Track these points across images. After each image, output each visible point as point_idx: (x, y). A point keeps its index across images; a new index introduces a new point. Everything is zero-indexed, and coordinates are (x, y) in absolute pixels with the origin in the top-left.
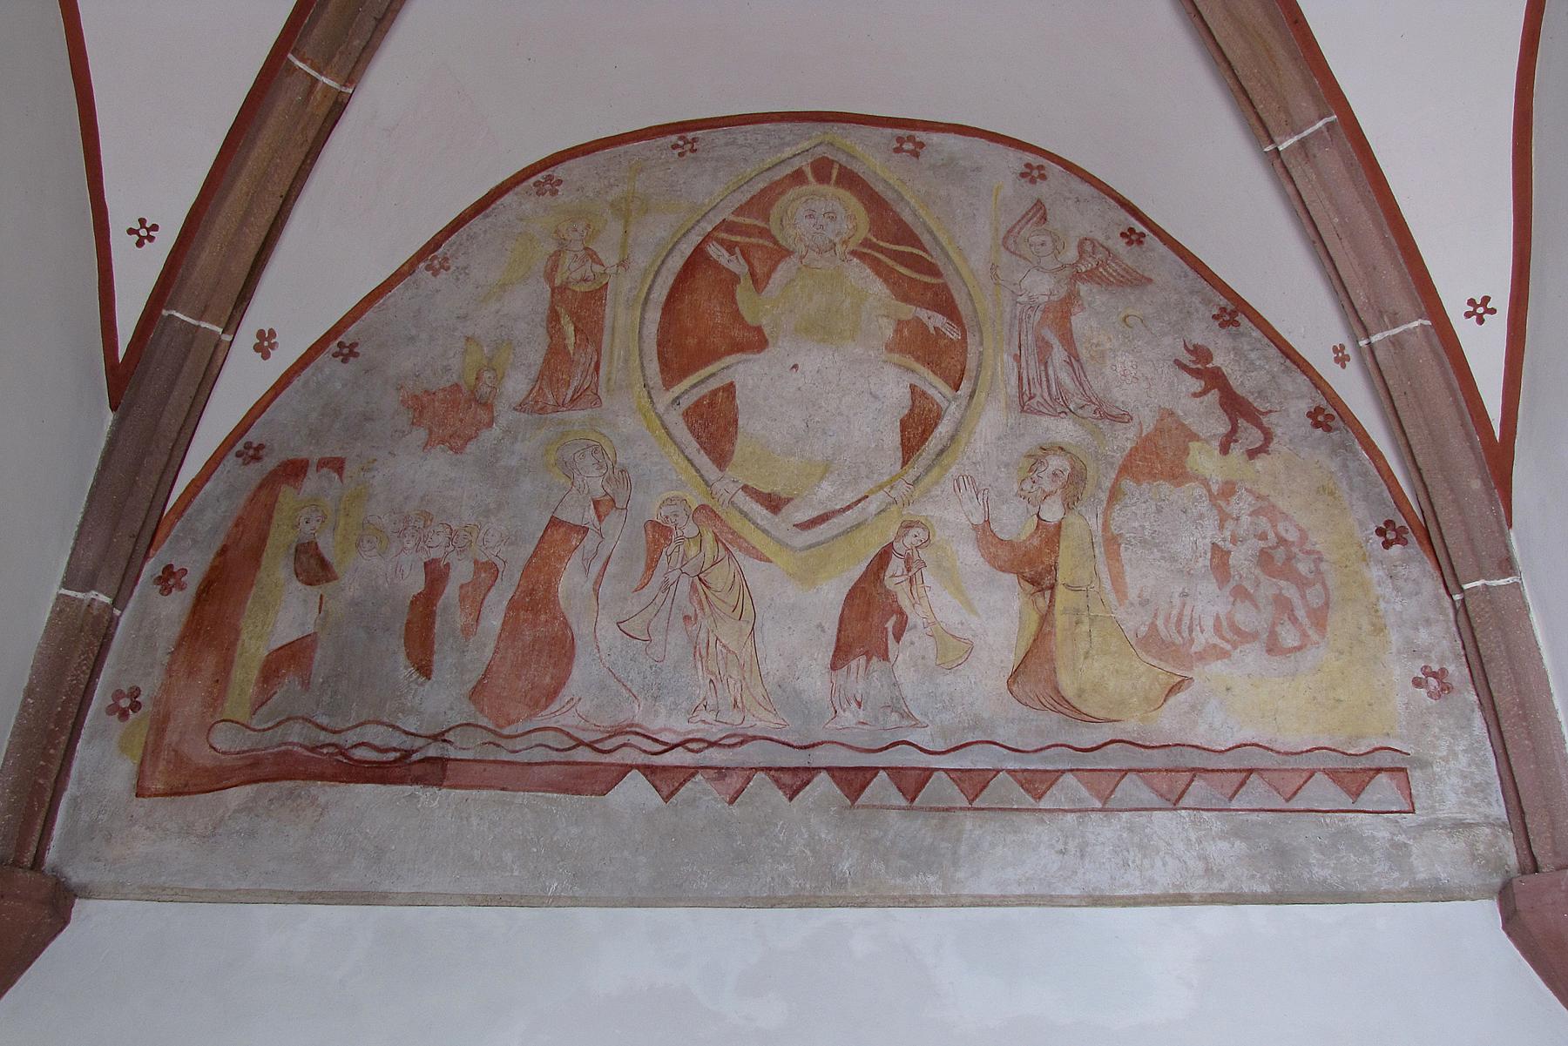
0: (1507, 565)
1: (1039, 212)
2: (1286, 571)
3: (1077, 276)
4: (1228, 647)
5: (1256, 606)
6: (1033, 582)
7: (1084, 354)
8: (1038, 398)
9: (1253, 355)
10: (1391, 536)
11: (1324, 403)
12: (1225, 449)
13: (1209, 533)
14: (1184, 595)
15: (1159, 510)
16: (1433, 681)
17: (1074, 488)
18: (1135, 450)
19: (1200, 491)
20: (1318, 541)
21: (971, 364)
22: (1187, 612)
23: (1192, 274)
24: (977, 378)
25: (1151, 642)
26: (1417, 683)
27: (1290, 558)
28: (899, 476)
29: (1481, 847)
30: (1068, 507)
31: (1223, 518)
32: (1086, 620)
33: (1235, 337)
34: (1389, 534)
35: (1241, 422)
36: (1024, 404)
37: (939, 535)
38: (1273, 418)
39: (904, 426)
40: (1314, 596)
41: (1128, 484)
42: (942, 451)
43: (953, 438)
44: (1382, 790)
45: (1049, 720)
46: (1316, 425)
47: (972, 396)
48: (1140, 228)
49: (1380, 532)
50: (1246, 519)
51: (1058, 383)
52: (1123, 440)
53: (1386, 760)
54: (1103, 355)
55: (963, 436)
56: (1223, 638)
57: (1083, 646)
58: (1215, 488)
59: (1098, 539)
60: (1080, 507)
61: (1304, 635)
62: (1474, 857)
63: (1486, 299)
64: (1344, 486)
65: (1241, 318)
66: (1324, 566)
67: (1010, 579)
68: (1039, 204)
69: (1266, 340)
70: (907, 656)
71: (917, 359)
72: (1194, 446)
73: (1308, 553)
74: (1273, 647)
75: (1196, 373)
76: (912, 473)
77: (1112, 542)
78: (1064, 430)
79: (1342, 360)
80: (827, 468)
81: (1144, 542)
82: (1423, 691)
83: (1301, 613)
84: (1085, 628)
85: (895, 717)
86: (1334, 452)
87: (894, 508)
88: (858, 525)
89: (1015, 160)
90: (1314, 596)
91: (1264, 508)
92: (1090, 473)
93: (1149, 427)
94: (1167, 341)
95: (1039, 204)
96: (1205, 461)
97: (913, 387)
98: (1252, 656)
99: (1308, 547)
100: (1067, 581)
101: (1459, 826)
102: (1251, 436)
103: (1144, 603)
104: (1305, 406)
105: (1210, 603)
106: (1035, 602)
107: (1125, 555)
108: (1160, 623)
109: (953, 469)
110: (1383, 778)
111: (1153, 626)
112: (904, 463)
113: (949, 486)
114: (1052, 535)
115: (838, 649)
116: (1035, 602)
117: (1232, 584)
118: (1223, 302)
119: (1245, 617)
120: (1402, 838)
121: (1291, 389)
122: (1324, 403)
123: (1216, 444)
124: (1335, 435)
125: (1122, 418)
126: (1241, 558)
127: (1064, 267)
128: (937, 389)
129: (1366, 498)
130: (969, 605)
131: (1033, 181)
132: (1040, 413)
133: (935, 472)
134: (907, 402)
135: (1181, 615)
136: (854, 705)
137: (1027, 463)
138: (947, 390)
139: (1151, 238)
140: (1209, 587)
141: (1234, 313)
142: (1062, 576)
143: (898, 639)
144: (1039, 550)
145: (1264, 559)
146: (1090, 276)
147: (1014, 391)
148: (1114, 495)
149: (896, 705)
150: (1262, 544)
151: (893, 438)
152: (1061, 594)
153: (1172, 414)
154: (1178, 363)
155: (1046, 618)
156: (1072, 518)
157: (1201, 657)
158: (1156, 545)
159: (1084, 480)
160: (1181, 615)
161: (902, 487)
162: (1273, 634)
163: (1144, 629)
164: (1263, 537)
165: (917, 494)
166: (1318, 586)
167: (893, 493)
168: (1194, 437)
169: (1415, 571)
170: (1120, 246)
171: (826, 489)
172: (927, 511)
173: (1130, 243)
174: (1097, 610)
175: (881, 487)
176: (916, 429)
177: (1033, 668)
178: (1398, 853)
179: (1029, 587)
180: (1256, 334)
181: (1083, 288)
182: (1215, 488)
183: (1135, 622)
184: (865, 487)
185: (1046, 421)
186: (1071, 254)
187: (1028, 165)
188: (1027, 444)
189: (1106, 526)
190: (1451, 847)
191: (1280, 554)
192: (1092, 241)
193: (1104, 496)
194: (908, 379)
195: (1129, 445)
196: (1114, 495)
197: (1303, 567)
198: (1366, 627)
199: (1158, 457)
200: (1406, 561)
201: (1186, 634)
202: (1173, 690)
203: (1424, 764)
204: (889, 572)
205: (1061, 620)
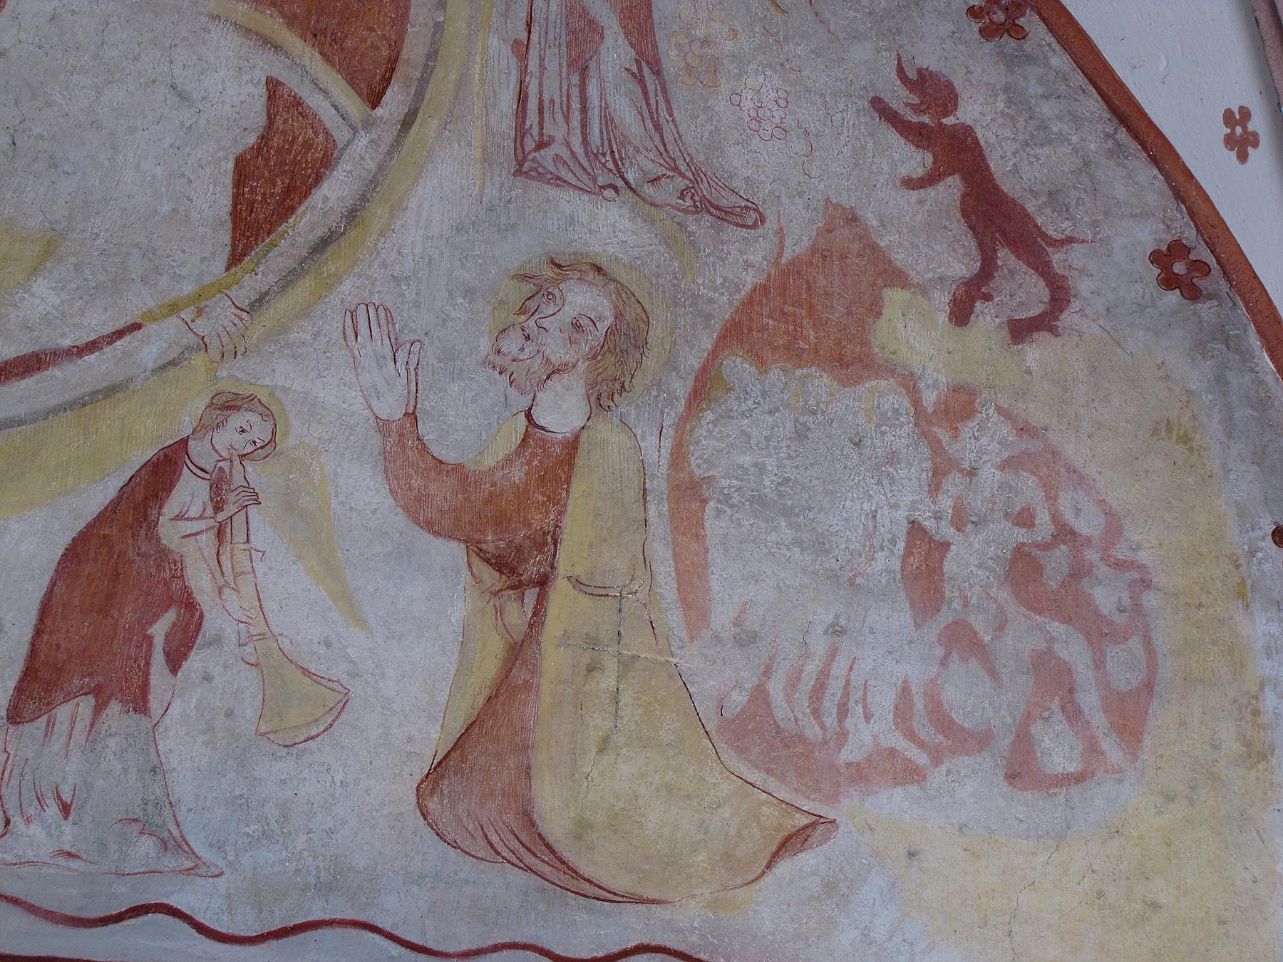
2: (1069, 604)
4: (922, 759)
5: (993, 673)
6: (500, 564)
7: (671, 59)
8: (557, 148)
9: (1047, 109)
11: (1190, 235)
12: (961, 313)
13: (904, 498)
14: (836, 630)
15: (801, 434)
17: (616, 360)
18: (761, 291)
19: (896, 400)
20: (1146, 542)
21: (414, 48)
22: (839, 669)
24: (423, 82)
25: (752, 730)
27: (1078, 573)
28: (220, 288)
30: (601, 399)
31: (941, 469)
32: (611, 665)
33: (1012, 62)
35: (1005, 256)
36: (526, 157)
37: (298, 433)
38: (1076, 255)
39: (243, 171)
40: (1123, 664)
41: (737, 366)
42: (323, 244)
43: (353, 216)
45: (505, 885)
46: (1169, 281)
47: (407, 122)
50: (990, 476)
51: (608, 120)
52: (740, 264)
54: (713, 66)
55: (378, 213)
56: (911, 736)
57: (598, 722)
58: (930, 398)
59: (658, 484)
60: (623, 406)
61: (1092, 748)
64: (1215, 425)
66: (1151, 600)
67: (450, 553)
69: (1078, 79)
70: (194, 709)
71: (291, 21)
72: (894, 298)
73: (1121, 565)
74: (1021, 770)
75: (917, 135)
76: (250, 284)
77: (689, 493)
78: (609, 228)
79: (1241, 144)
80: (50, 248)
81: (759, 500)
83: (1089, 700)
84: (607, 681)
85: (147, 846)
86: (1200, 348)
87: (198, 360)
88: (111, 391)
90: (1123, 664)
91: (1035, 455)
92: (657, 332)
93: (798, 244)
94: (861, 53)
96: (914, 332)
97: (273, 87)
98: (971, 786)
99: (1121, 553)
100: (579, 571)
102: (1022, 290)
103: (745, 639)
104: (1148, 236)
105: (890, 656)
106: (499, 612)
107: (714, 526)
108: (776, 688)
109: (346, 287)
111: (760, 695)
112: (235, 259)
113: (334, 323)
114: (555, 464)
115: (30, 674)
116: (499, 612)
117: (946, 616)
119: (966, 694)
121: (1120, 192)
122: (1190, 235)
123: (942, 299)
124: (1206, 310)
125: (741, 215)
126: (971, 561)
128: (328, 96)
130: (347, 601)
132: (559, 181)
133: (303, 288)
134: (256, 117)
135: (824, 674)
136: (53, 811)
137: (516, 293)
138: (353, 104)
140: (894, 617)
142: (569, 559)
143: (175, 661)
144: (522, 494)
145: (1022, 569)
147: (504, 124)
148: (706, 387)
149: (155, 821)
150: (1020, 535)
151: (213, 199)
152: (561, 595)
153: (852, 218)
155: (520, 651)
156: (604, 430)
157: (860, 774)
158: (786, 512)
159: (641, 345)
160: (824, 674)
161: (222, 315)
162: (1024, 742)
163: (738, 699)
164: (1025, 519)
165: (255, 335)
166: (1135, 644)
167: (202, 326)
168: (897, 277)
171: (43, 296)
172: (277, 375)
174: (639, 644)
175: (174, 308)
176: (272, 180)
177: (481, 758)
179: (489, 576)
180: (1060, 61)
182: (930, 398)
183: (719, 680)
184: (135, 303)
185: (569, 202)
188: (520, 250)
189: (678, 457)
191: (1057, 563)
193: (681, 388)
194: (265, 64)
195: (750, 280)
196: (706, 387)
197: (1106, 596)
198: (1230, 744)
199: (810, 314)
201: (830, 721)
202: (792, 842)
204: (172, 506)
205: (555, 659)
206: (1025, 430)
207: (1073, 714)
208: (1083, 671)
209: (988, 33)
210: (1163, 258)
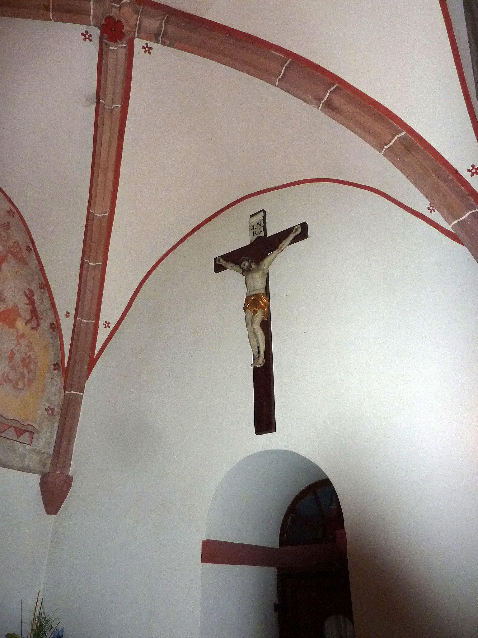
0: (82, 390)
1: (7, 226)
3: (9, 252)
9: (44, 300)
10: (56, 367)
12: (26, 324)
13: (12, 346)
16: (50, 411)
18: (3, 312)
20: (39, 361)
23: (39, 269)
26: (46, 410)
27: (30, 362)
29: (43, 459)
33: (42, 293)
34: (56, 366)
35: (34, 318)
38: (42, 321)
44: (25, 437)
46: (51, 328)
48: (32, 247)
49: (55, 365)
53: (30, 428)
58: (19, 334)
62: (40, 462)
63: (109, 323)
65: (46, 288)
66: (37, 369)
68: (8, 223)
72: (19, 319)
74: (15, 387)
75: (29, 298)
79: (67, 315)
82: (47, 413)
83: (26, 379)
86: (52, 338)
89: (8, 206)
94: (24, 284)
95: (8, 223)
96: (20, 325)
101: (40, 453)
110: (27, 434)
117: (12, 364)
118: (43, 281)
120: (25, 452)
123: (25, 321)
124: (54, 333)
126: (18, 357)
127: (7, 247)
129: (55, 354)
131: (10, 215)
139: (33, 252)
140: (6, 362)
141: (45, 286)
145: (23, 360)
146: (13, 254)
154: (25, 292)
164: (26, 353)
168: (20, 316)
169: (58, 379)
170: (24, 249)
173: (27, 250)
178: (23, 456)
180: (47, 295)
181: (10, 257)
182: (19, 334)
186: (11, 244)
187: (11, 210)
190: (36, 457)
191: (27, 360)
192: (18, 244)
197: (32, 367)
200: (57, 376)
203: (38, 432)
206: (29, 342)
207: (24, 381)
208: (27, 376)
209: (41, 288)
210: (52, 325)
